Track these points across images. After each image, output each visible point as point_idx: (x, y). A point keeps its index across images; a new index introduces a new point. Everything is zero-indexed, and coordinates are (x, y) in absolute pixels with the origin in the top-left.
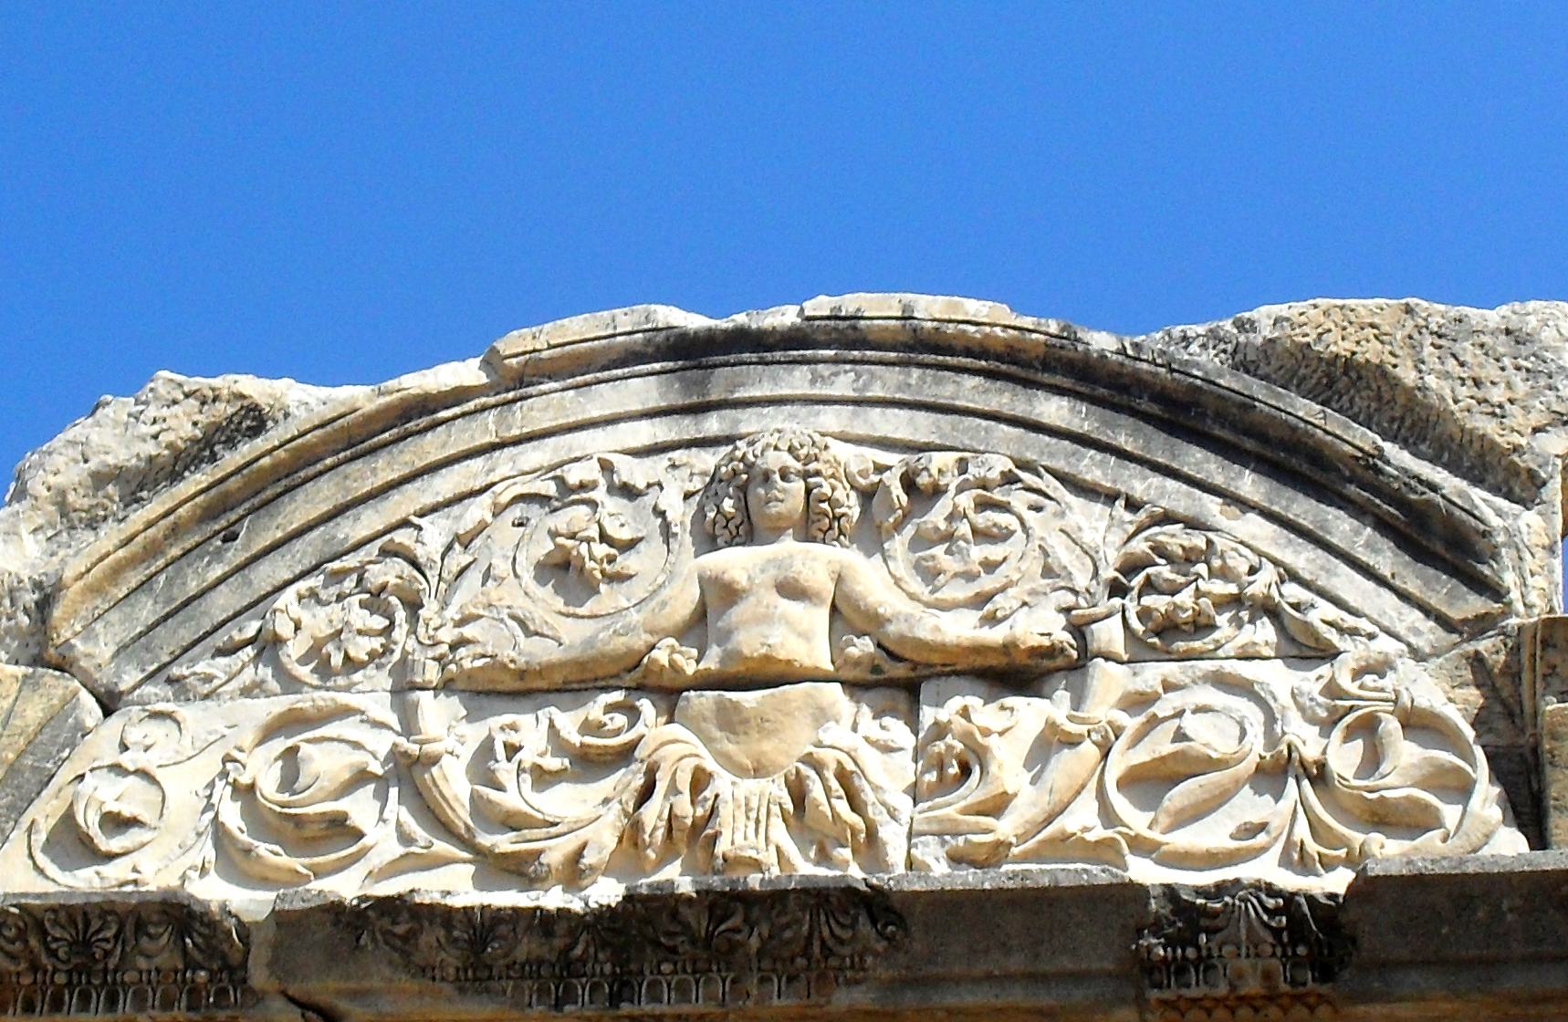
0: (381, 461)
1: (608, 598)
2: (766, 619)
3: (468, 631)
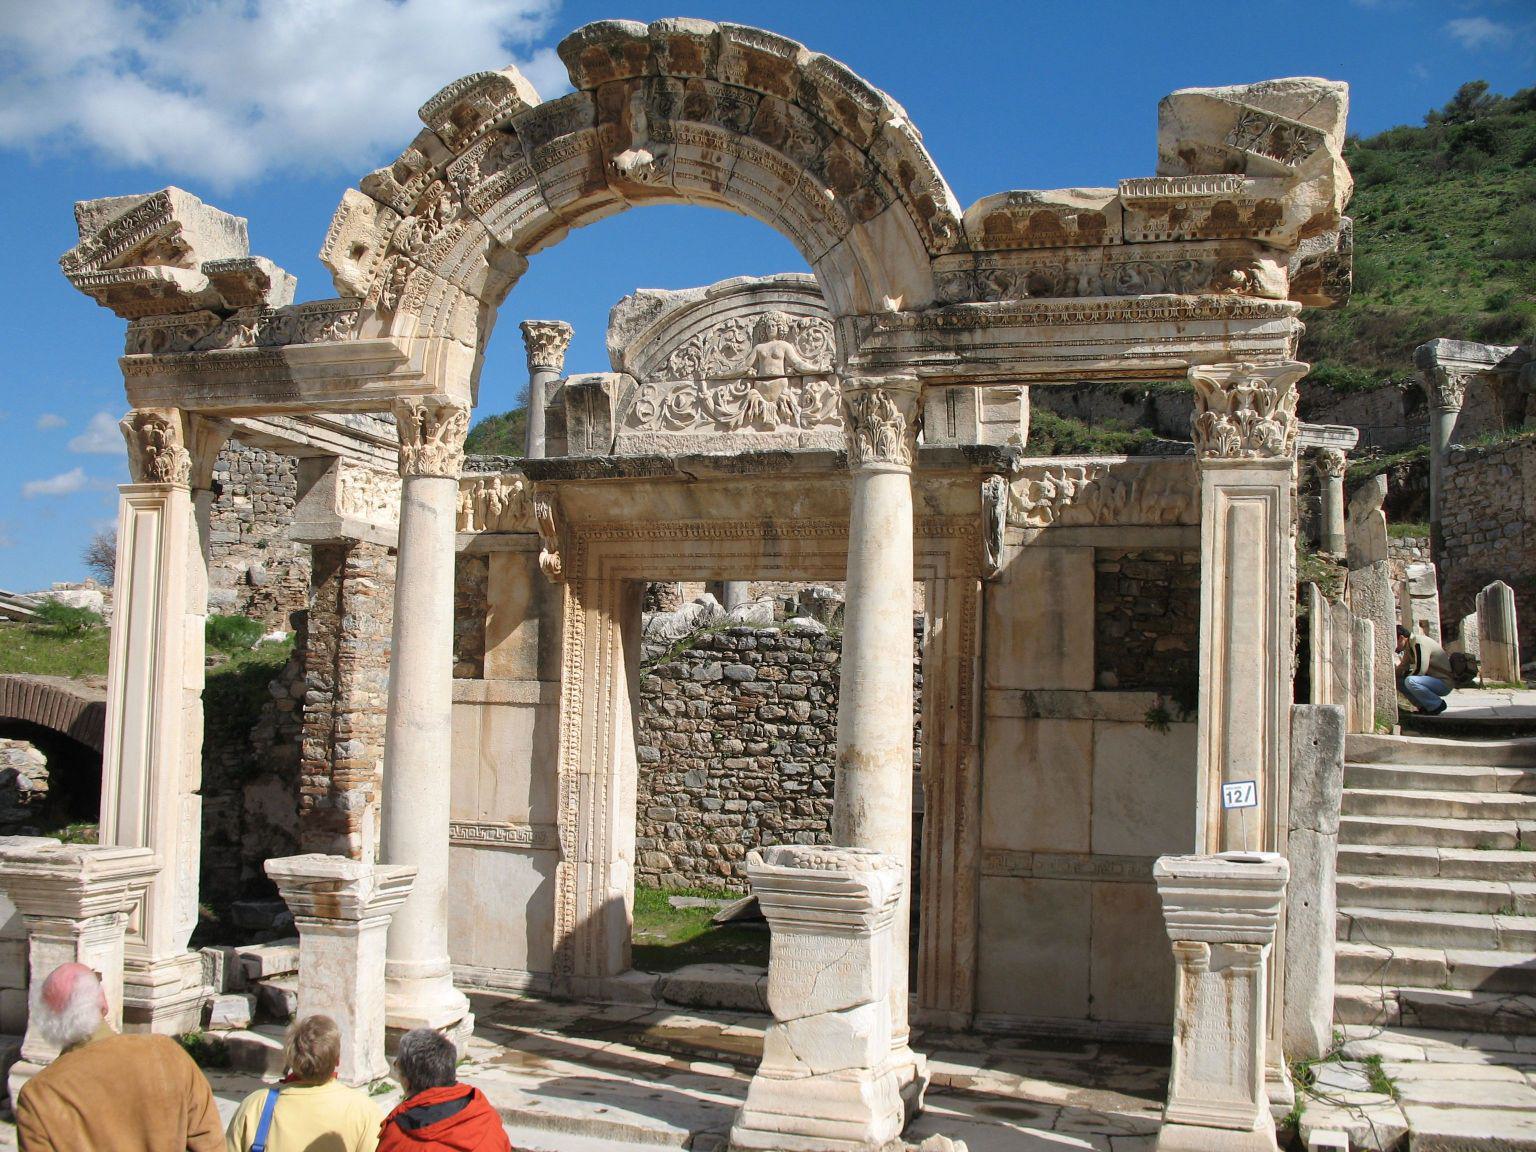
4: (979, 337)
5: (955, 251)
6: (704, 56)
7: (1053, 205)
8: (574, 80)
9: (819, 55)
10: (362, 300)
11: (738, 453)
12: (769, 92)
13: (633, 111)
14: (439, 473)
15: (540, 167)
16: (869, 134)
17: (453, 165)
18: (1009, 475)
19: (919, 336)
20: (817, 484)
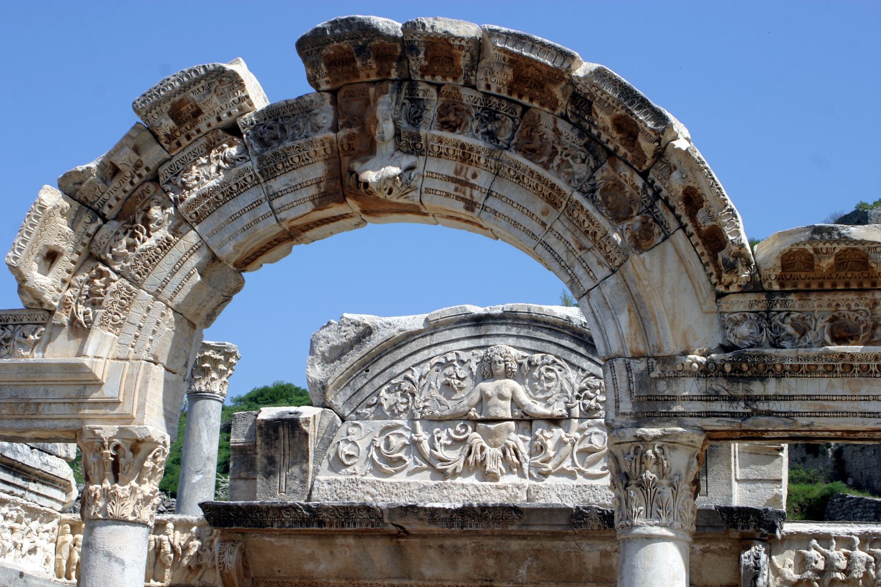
0: (402, 350)
1: (460, 395)
2: (496, 405)
3: (427, 404)
4: (772, 387)
5: (744, 290)
6: (463, 61)
7: (862, 242)
8: (313, 81)
9: (594, 66)
10: (51, 312)
11: (459, 505)
12: (535, 104)
13: (379, 116)
14: (131, 518)
15: (268, 172)
16: (649, 155)
17: (166, 166)
18: (773, 544)
19: (702, 383)
20: (548, 544)
